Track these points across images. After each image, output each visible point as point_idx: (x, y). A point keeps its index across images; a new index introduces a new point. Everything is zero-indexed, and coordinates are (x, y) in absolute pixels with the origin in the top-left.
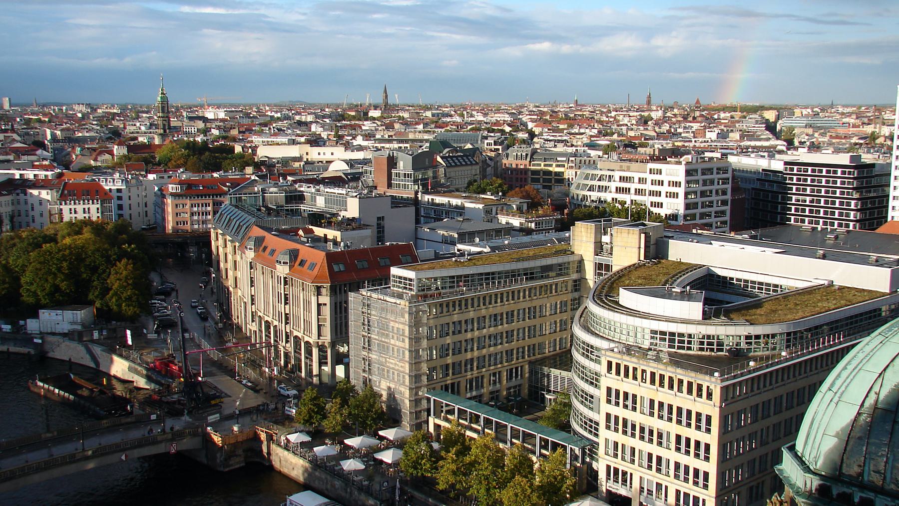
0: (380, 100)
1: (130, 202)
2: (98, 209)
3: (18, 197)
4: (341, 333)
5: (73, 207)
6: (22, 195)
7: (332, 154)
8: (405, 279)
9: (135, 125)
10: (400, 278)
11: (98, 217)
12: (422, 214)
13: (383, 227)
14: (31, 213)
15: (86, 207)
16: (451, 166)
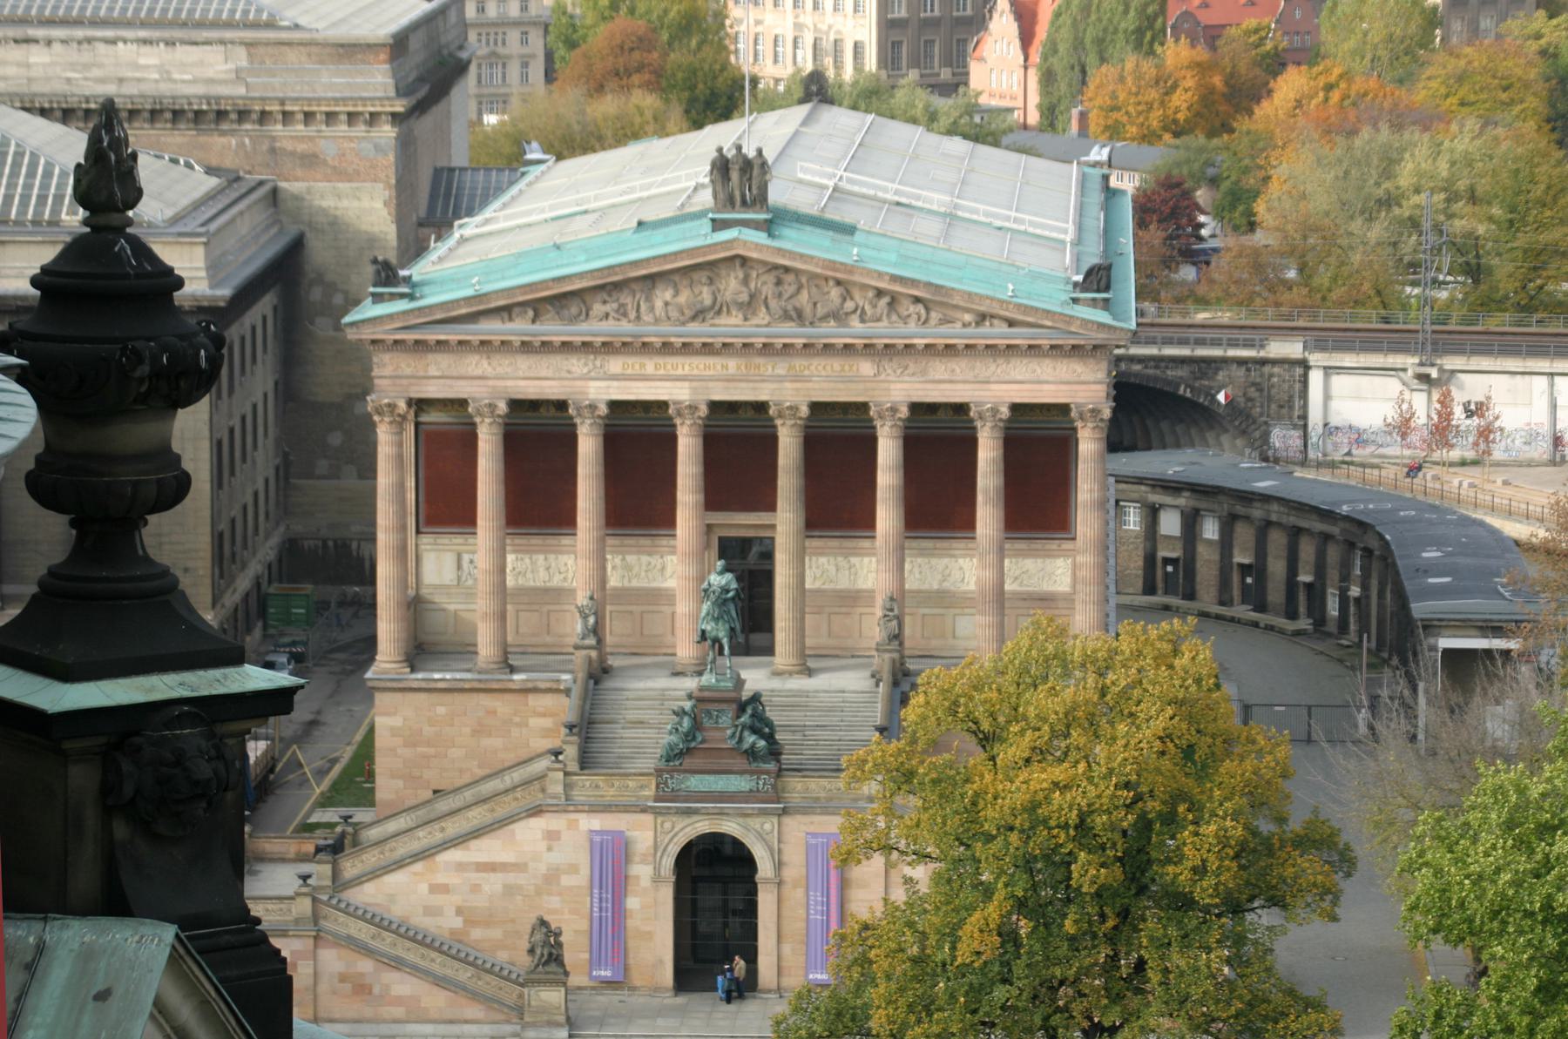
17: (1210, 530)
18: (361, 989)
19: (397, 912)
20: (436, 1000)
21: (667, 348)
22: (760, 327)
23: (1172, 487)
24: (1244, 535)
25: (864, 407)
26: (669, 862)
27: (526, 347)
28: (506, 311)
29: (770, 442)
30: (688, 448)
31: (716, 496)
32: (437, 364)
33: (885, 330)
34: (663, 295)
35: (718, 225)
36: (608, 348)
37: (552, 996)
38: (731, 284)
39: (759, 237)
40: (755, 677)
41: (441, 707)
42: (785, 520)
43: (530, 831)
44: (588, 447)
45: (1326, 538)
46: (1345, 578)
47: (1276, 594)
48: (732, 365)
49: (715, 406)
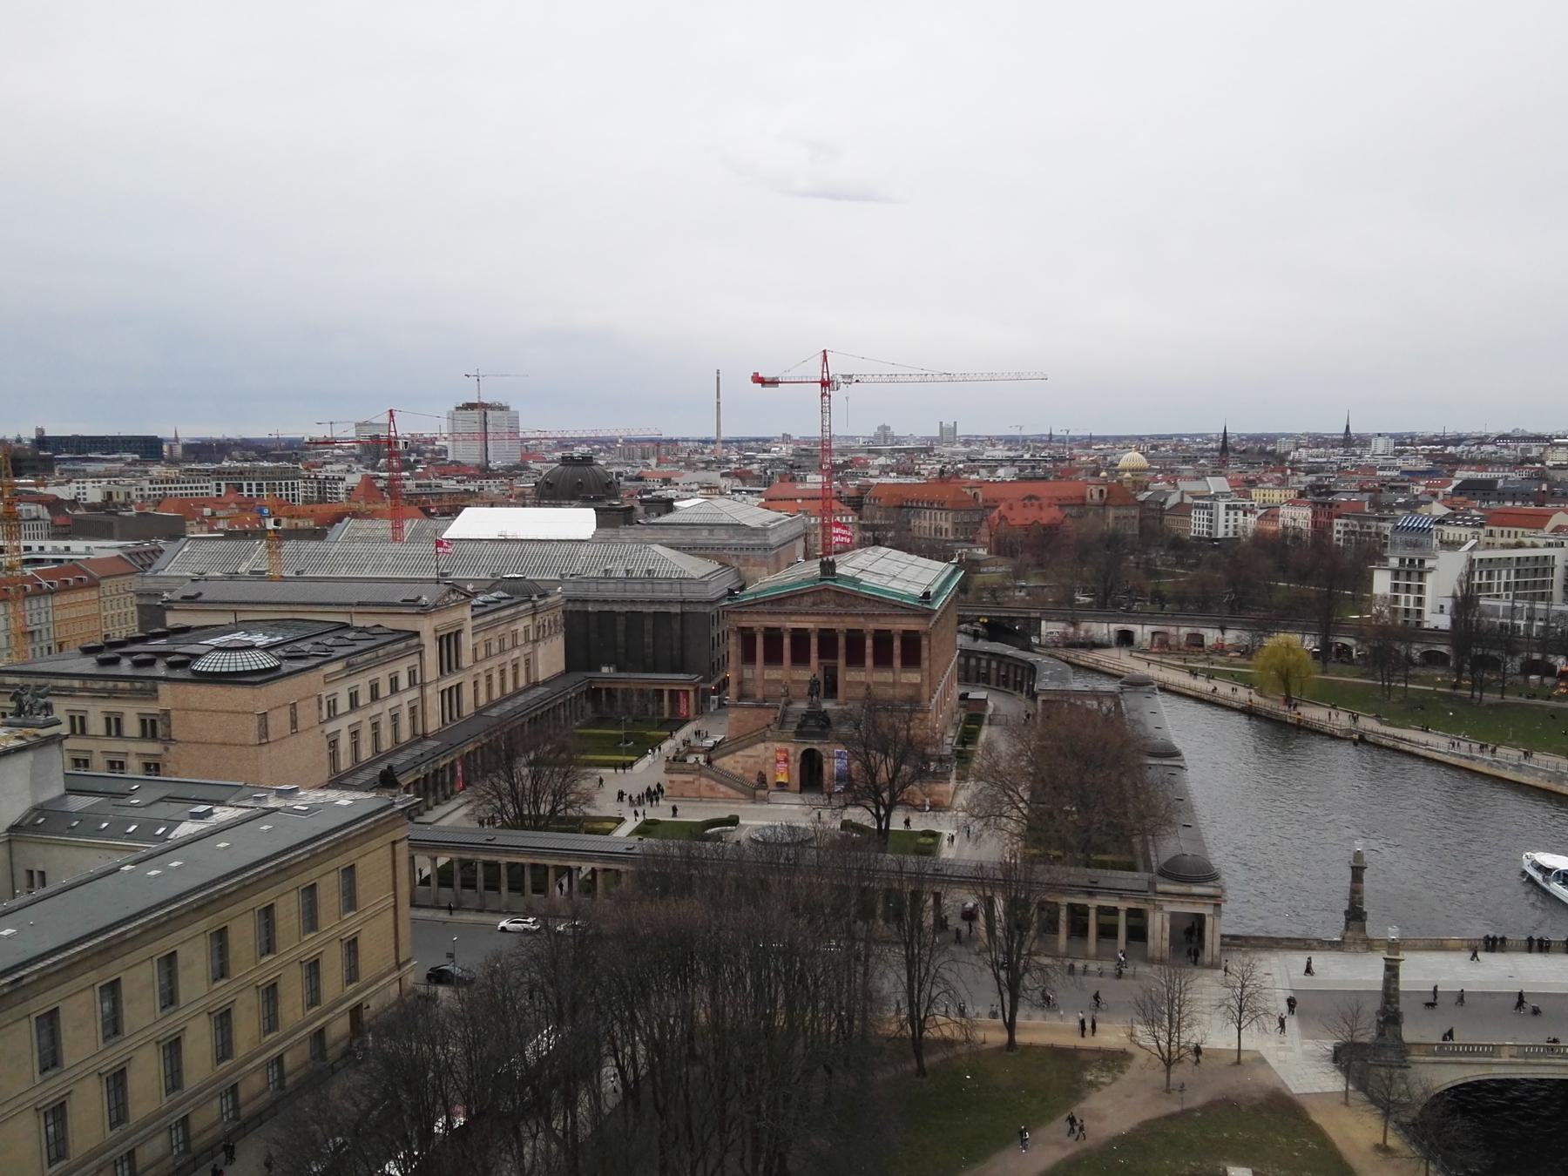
21: (807, 614)
22: (832, 607)
27: (769, 613)
28: (764, 603)
29: (836, 640)
30: (814, 642)
31: (821, 655)
32: (745, 617)
34: (805, 598)
35: (821, 580)
36: (791, 614)
38: (826, 597)
39: (832, 583)
40: (827, 705)
42: (841, 661)
44: (787, 641)
46: (1029, 679)
48: (825, 619)
49: (821, 630)
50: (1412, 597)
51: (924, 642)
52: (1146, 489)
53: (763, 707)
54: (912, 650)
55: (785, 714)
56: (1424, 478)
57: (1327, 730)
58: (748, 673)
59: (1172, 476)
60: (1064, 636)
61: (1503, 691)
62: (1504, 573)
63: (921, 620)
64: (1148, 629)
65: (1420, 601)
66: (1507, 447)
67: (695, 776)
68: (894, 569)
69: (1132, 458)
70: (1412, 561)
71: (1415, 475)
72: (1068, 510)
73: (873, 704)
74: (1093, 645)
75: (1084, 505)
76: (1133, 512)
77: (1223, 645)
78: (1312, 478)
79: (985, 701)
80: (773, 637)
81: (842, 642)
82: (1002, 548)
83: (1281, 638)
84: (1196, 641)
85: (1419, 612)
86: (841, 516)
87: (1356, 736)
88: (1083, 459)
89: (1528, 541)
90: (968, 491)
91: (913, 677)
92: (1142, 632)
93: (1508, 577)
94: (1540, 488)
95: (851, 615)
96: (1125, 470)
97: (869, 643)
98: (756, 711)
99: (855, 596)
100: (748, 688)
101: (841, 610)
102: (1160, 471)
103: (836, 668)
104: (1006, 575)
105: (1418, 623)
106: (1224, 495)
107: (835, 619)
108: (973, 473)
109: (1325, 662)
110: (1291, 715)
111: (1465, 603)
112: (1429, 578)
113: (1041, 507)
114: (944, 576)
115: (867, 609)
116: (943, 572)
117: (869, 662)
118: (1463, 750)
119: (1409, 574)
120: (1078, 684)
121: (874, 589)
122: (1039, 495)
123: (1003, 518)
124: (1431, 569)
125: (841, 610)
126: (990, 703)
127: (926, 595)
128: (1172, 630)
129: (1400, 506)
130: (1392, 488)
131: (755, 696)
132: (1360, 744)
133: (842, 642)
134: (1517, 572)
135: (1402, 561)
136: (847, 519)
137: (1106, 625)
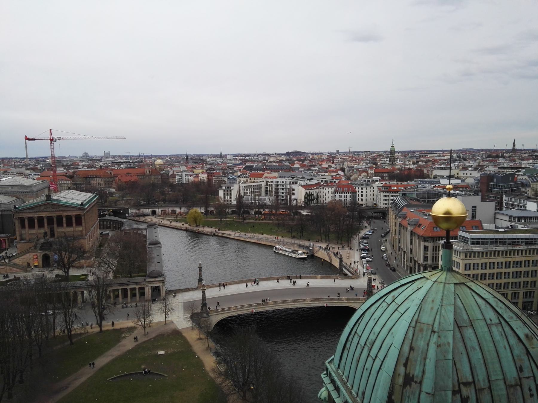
0: (510, 147)
1: (366, 194)
2: (350, 196)
3: (321, 190)
4: (436, 261)
5: (340, 195)
6: (322, 189)
7: (471, 174)
8: (465, 238)
9: (384, 160)
10: (463, 237)
11: (350, 200)
12: (504, 206)
13: (476, 211)
14: (325, 197)
15: (346, 195)
16: (534, 182)
17: (112, 223)
18: (11, 270)
19: (16, 263)
20: (18, 270)
21: (42, 212)
22: (51, 209)
23: (108, 220)
24: (114, 224)
25: (61, 216)
26: (41, 256)
27: (29, 212)
29: (53, 219)
30: (45, 220)
31: (48, 224)
32: (20, 214)
33: (63, 209)
34: (41, 207)
35: (46, 201)
36: (37, 212)
37: (29, 269)
41: (23, 244)
42: (55, 226)
43: (28, 255)
44: (36, 221)
45: (120, 223)
47: (117, 228)
48: (49, 213)
49: (47, 216)
50: (229, 196)
51: (83, 218)
52: (163, 170)
53: (29, 242)
54: (79, 221)
55: (36, 244)
56: (238, 166)
57: (206, 233)
58: (23, 232)
59: (172, 166)
60: (136, 213)
61: (249, 219)
62: (250, 189)
63: (81, 211)
64: (160, 210)
65: (231, 198)
66: (260, 157)
67: (4, 266)
68: (74, 196)
69: (159, 161)
70: (228, 187)
71: (236, 165)
72: (140, 177)
73: (66, 237)
74: (144, 215)
75: (145, 175)
76: (159, 177)
77: (181, 213)
78: (210, 166)
79: (108, 234)
80: (31, 220)
81: (55, 219)
82: (120, 188)
83: (195, 209)
84: (174, 212)
85: (231, 201)
86: (60, 181)
87: (213, 234)
88: (148, 162)
89: (256, 181)
90: (108, 172)
91: (80, 229)
92: (158, 211)
93: (251, 190)
94: (263, 167)
95: (57, 211)
96: (157, 165)
97: (64, 219)
98: (27, 243)
99: (58, 205)
100: (24, 236)
101: (54, 210)
102: (169, 165)
103: (54, 228)
104: (119, 197)
105: (231, 203)
106: (184, 171)
107: (52, 213)
108: (113, 166)
109: (207, 215)
110: (197, 229)
111: (239, 198)
112: (232, 191)
113: (131, 176)
114: (91, 198)
115: (63, 209)
116: (90, 196)
117: (65, 225)
118: (241, 235)
119: (227, 191)
120: (135, 226)
121: (65, 203)
122: (131, 173)
123: (119, 180)
124: (233, 189)
125: (54, 210)
126: (110, 235)
127: (82, 203)
128: (167, 209)
129: (230, 173)
130: (230, 168)
131: (26, 239)
132: (214, 236)
133: (55, 219)
134: (254, 189)
135: (226, 187)
136: (66, 182)
137: (148, 209)
